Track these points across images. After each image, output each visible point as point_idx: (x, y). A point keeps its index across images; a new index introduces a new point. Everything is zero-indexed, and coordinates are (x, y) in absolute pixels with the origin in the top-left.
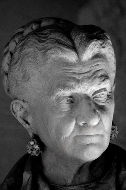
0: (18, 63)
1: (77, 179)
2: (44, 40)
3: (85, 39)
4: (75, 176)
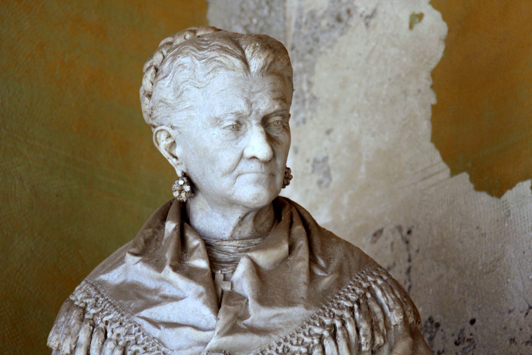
0: (168, 77)
1: (237, 233)
2: (206, 47)
3: (259, 49)
4: (235, 229)
